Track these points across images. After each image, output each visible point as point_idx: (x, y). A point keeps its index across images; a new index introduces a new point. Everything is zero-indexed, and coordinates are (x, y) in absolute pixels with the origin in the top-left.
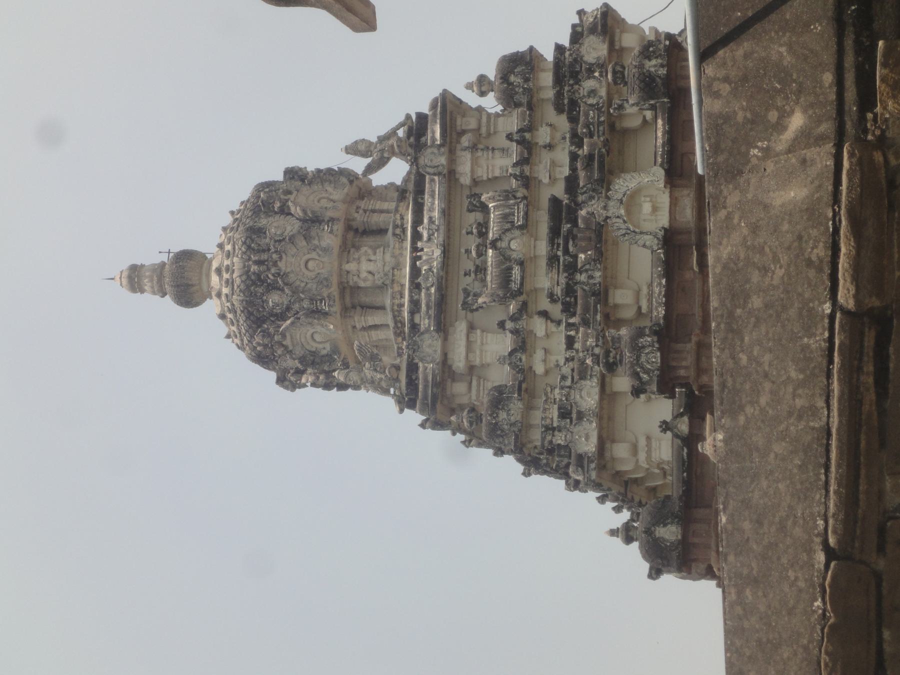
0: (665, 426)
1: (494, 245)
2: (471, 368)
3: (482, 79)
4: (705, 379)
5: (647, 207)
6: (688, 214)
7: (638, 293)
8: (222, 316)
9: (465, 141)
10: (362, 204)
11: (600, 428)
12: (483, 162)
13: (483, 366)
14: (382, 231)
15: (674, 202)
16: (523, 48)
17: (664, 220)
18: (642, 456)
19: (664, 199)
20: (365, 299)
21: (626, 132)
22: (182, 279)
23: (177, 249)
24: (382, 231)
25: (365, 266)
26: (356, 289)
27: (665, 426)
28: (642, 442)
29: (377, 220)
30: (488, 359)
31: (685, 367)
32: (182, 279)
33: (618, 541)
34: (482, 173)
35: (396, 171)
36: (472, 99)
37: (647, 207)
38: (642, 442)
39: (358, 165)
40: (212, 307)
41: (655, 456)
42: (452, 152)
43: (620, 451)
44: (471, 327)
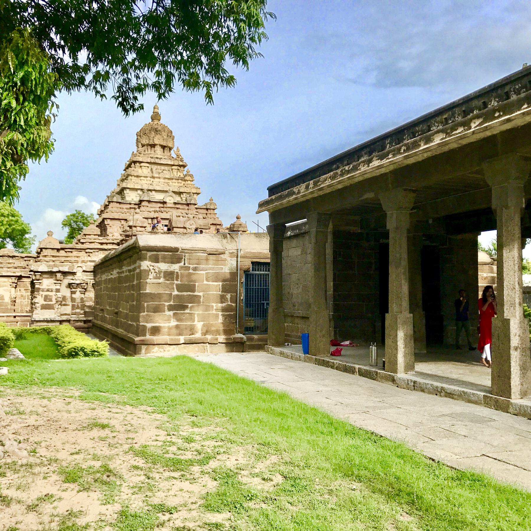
0: (133, 199)
6: (168, 205)
9: (179, 168)
15: (171, 203)
34: (174, 170)
36: (186, 169)
39: (175, 149)
43: (128, 191)
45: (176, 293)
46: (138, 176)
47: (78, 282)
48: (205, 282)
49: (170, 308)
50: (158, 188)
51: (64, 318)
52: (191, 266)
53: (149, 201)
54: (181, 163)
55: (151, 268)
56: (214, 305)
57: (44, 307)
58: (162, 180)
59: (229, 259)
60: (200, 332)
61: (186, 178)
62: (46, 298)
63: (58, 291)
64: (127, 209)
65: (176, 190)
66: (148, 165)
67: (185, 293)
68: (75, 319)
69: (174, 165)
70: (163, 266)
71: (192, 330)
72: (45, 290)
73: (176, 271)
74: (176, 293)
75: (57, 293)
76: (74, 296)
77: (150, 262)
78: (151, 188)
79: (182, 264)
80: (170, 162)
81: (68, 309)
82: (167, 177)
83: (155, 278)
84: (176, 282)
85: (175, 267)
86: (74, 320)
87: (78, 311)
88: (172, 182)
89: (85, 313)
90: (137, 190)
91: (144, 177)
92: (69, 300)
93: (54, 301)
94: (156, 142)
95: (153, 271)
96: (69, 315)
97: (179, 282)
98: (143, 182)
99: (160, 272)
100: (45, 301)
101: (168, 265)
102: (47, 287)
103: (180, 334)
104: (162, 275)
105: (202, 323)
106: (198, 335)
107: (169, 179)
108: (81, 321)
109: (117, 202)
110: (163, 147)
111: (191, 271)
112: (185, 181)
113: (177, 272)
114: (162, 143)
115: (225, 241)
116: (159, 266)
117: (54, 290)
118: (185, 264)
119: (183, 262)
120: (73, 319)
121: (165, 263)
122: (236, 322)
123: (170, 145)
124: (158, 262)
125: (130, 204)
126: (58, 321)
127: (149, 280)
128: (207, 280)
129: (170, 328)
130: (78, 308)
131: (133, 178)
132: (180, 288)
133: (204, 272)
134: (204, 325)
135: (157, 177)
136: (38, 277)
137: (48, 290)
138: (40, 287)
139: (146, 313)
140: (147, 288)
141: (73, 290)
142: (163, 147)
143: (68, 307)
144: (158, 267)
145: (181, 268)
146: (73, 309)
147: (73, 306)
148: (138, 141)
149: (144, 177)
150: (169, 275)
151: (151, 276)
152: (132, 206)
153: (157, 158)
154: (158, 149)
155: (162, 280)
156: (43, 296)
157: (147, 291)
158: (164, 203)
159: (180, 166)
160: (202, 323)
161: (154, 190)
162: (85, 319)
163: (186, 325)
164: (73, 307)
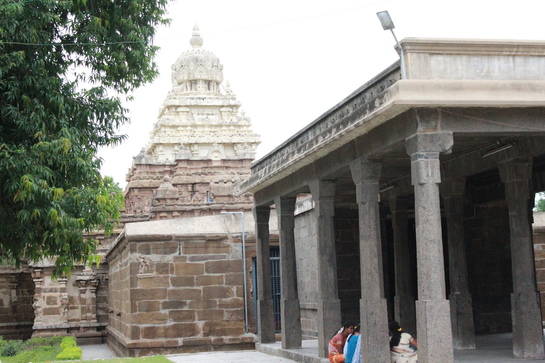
0: (167, 159)
1: (207, 117)
2: (178, 112)
3: (244, 113)
4: (179, 169)
5: (216, 155)
6: (215, 164)
7: (197, 151)
8: (188, 51)
9: (230, 109)
10: (215, 84)
11: (166, 144)
12: (226, 113)
13: (179, 115)
14: (209, 90)
15: (218, 161)
16: (251, 123)
17: (213, 159)
18: (160, 153)
19: (219, 159)
20: (193, 85)
21: (233, 147)
22: (196, 41)
23: (203, 39)
24: (209, 90)
25: (201, 86)
26: (196, 83)
27: (167, 159)
28: (163, 153)
29: (212, 88)
30: (180, 116)
31: (181, 165)
32: (196, 41)
33: (141, 150)
34: (223, 113)
35: (223, 92)
36: (240, 110)
37: (216, 155)
38: (163, 153)
40: (190, 48)
41: (160, 156)
42: (228, 106)
43: (161, 148)
44: (188, 112)
45: (171, 288)
46: (173, 127)
47: (87, 278)
48: (205, 274)
49: (166, 306)
50: (202, 140)
51: (73, 324)
52: (188, 256)
53: (188, 161)
54: (232, 103)
55: (142, 260)
56: (217, 300)
57: (47, 312)
58: (207, 129)
59: (232, 245)
60: (202, 332)
61: (241, 123)
62: (50, 301)
63: (63, 290)
64: (160, 173)
65: (226, 141)
66: (188, 110)
67: (182, 288)
68: (86, 325)
69: (223, 106)
70: (155, 258)
71: (193, 330)
72: (48, 290)
73: (170, 262)
74: (171, 288)
75: (63, 294)
76: (83, 296)
77: (140, 254)
78: (192, 141)
79: (177, 254)
80: (220, 103)
81: (77, 314)
82: (213, 123)
83: (145, 272)
84: (170, 275)
85: (169, 258)
86: (84, 328)
87: (89, 315)
88: (222, 131)
89: (98, 318)
90: (174, 145)
91: (183, 126)
92: (78, 301)
93: (59, 304)
94: (197, 76)
95: (143, 264)
96: (78, 320)
97: (174, 276)
98: (181, 133)
99: (152, 265)
100: (48, 303)
101: (161, 256)
102: (50, 287)
103: (179, 336)
104: (154, 268)
105: (204, 322)
106: (200, 336)
107: (216, 126)
108: (93, 328)
109: (147, 165)
110: (208, 83)
111: (188, 262)
112: (239, 126)
113: (172, 264)
114: (205, 77)
115: (228, 223)
116: (150, 258)
117: (59, 290)
118: (180, 254)
119: (178, 252)
120: (83, 325)
121: (157, 254)
122: (245, 319)
123: (218, 79)
124: (148, 253)
125: (164, 165)
126: (65, 329)
127: (139, 274)
128: (207, 271)
129: (166, 329)
130: (89, 311)
131: (167, 129)
132: (175, 282)
133: (203, 262)
134: (206, 324)
135: (200, 126)
136: (38, 274)
137: (51, 291)
138: (42, 287)
139: (138, 312)
140: (138, 283)
141: (82, 288)
142: (208, 83)
143: (77, 310)
144: (149, 259)
145: (176, 258)
146: (83, 313)
147: (83, 309)
148: (174, 78)
149: (183, 126)
150: (163, 268)
151: (141, 271)
152: (167, 169)
153: (199, 98)
154: (201, 87)
155: (154, 274)
156: (46, 298)
157: (139, 288)
158: (209, 161)
159: (232, 107)
160: (204, 322)
161: (196, 144)
162: (98, 325)
163: (185, 325)
164: (83, 310)
